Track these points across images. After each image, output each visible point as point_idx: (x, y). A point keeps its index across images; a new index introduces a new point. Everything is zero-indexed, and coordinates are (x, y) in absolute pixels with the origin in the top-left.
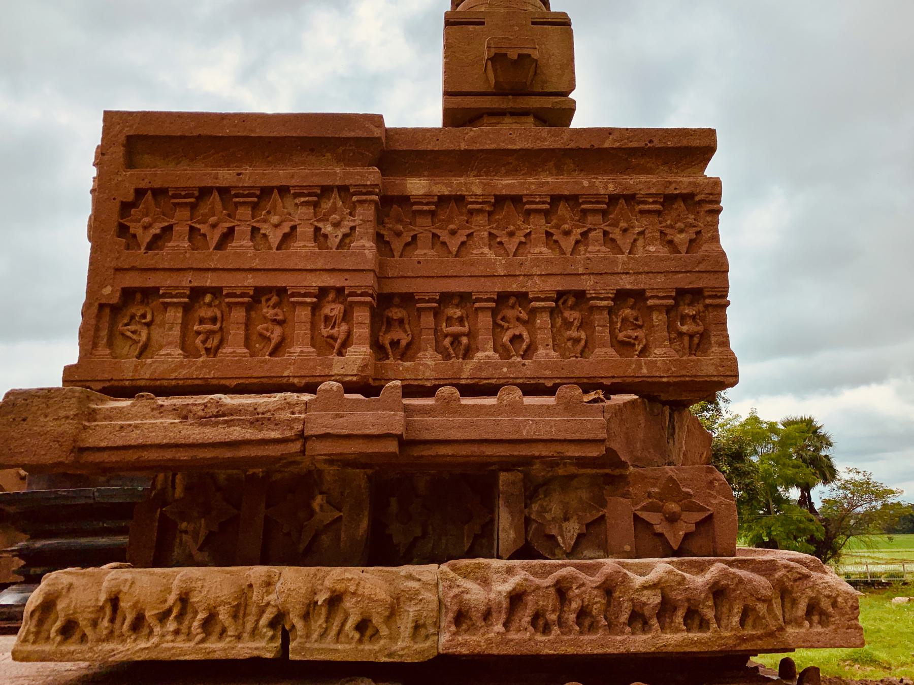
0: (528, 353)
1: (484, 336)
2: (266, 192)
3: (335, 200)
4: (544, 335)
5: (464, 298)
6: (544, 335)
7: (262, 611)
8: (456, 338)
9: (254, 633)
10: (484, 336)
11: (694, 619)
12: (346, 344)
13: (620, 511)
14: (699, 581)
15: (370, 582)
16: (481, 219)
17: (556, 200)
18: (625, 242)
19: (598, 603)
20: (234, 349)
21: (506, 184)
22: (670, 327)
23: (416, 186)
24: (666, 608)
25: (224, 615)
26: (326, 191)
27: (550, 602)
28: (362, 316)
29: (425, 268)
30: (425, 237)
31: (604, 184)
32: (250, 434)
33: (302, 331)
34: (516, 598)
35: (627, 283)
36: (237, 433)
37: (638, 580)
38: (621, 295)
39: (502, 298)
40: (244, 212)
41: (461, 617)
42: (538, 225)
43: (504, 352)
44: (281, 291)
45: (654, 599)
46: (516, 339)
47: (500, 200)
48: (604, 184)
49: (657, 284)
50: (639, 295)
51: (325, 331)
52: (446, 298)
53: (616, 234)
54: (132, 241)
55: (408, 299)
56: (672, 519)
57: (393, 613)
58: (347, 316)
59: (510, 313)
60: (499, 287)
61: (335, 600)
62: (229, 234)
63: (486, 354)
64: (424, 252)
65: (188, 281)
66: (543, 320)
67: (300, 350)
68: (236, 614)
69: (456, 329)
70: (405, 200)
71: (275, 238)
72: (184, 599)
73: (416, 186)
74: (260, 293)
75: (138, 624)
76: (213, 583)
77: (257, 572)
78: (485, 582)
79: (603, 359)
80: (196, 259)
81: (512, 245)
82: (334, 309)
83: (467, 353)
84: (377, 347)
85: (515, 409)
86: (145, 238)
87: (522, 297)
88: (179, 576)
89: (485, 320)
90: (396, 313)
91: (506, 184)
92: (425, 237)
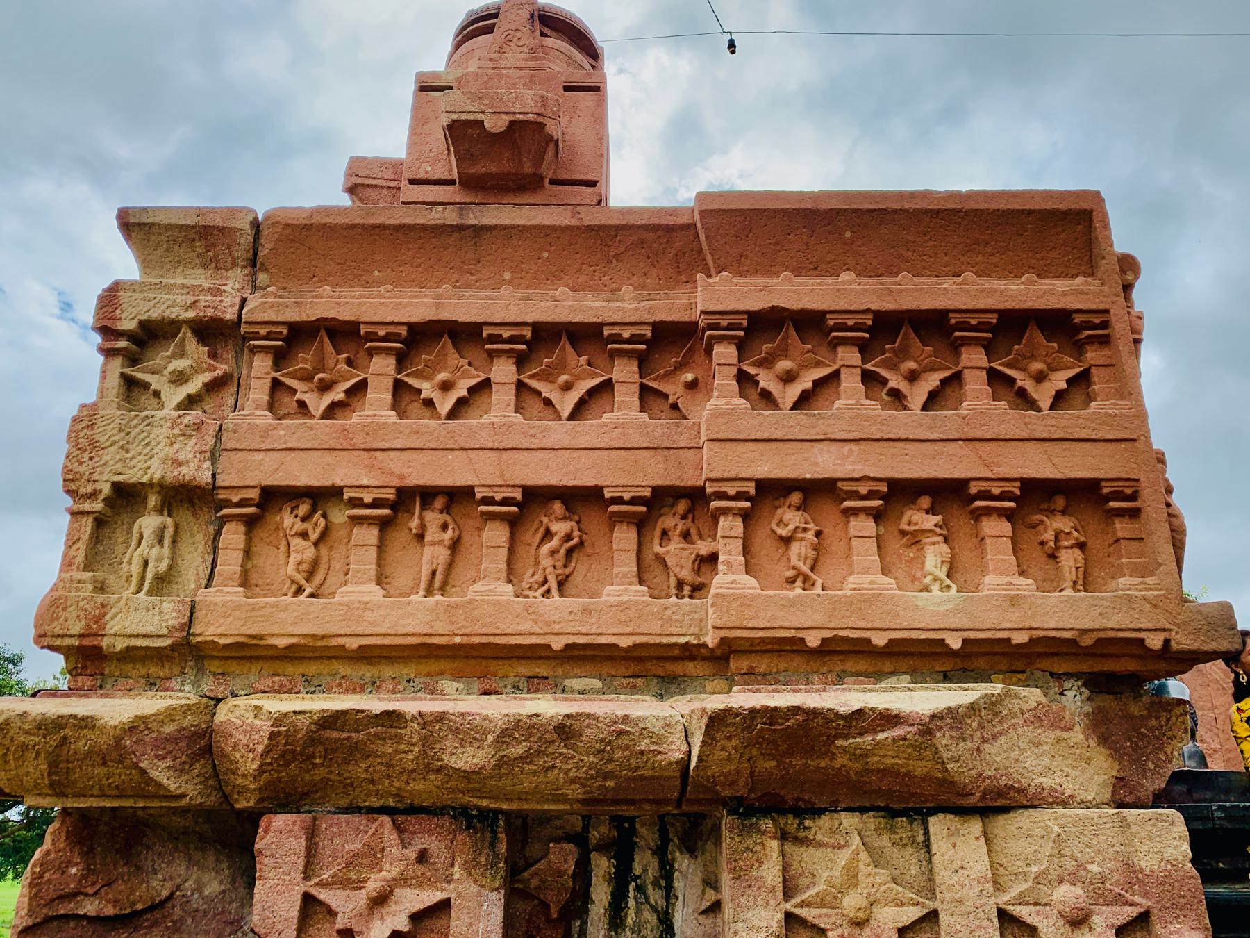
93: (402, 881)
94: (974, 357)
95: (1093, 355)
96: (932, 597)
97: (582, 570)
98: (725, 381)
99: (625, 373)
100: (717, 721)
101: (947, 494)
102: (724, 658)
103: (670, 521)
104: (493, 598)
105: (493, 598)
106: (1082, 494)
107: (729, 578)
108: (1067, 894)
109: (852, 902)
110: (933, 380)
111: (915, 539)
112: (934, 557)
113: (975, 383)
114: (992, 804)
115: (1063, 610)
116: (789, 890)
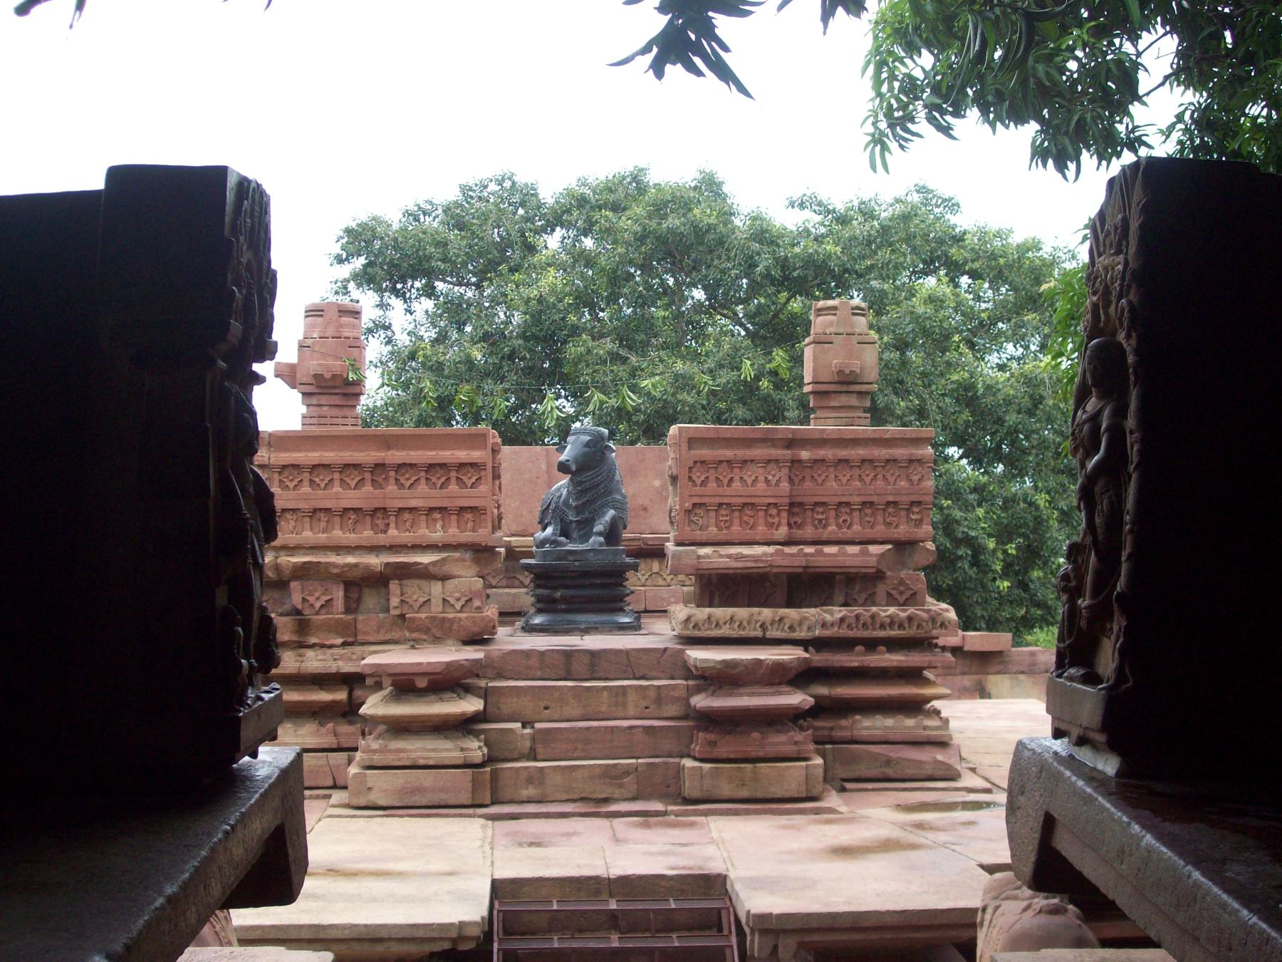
0: (849, 527)
1: (832, 520)
2: (745, 462)
3: (772, 465)
4: (856, 520)
5: (823, 504)
6: (856, 520)
7: (757, 622)
8: (820, 521)
9: (755, 629)
10: (832, 520)
11: (901, 626)
12: (779, 525)
13: (881, 589)
14: (903, 615)
15: (792, 614)
16: (832, 469)
17: (863, 461)
18: (892, 480)
19: (869, 621)
20: (736, 528)
21: (843, 453)
22: (908, 516)
23: (805, 454)
24: (891, 624)
25: (745, 623)
26: (769, 461)
27: (853, 621)
28: (784, 514)
29: (809, 490)
30: (808, 478)
31: (883, 453)
32: (753, 565)
33: (761, 521)
34: (842, 620)
35: (891, 499)
36: (749, 564)
37: (883, 614)
38: (888, 503)
39: (840, 504)
40: (737, 471)
41: (824, 625)
42: (856, 471)
43: (838, 525)
44: (752, 504)
45: (888, 620)
46: (845, 521)
47: (840, 461)
48: (883, 453)
49: (905, 499)
50: (895, 503)
51: (771, 520)
52: (816, 504)
53: (888, 476)
54: (694, 484)
55: (801, 504)
56: (901, 593)
57: (800, 624)
58: (778, 515)
59: (843, 510)
60: (838, 500)
61: (781, 619)
62: (731, 480)
63: (832, 528)
64: (808, 484)
65: (717, 500)
66: (856, 514)
67: (761, 528)
68: (749, 623)
69: (820, 517)
70: (800, 461)
71: (749, 481)
72: (732, 618)
73: (805, 454)
74: (745, 504)
75: (717, 625)
76: (742, 613)
77: (756, 610)
78: (832, 614)
79: (880, 530)
80: (721, 491)
81: (844, 481)
82: (774, 512)
83: (825, 527)
84: (789, 525)
85: (845, 554)
86: (699, 482)
87: (848, 504)
88: (730, 611)
89: (832, 513)
90: (796, 510)
91: (843, 453)
92: (808, 478)
93: (323, 594)
94: (453, 474)
95: (483, 473)
96: (437, 534)
97: (359, 526)
98: (392, 481)
99: (368, 476)
100: (387, 564)
101: (442, 510)
102: (393, 548)
103: (379, 515)
104: (339, 535)
105: (339, 535)
106: (473, 509)
107: (393, 532)
108: (457, 595)
109: (415, 597)
110: (443, 480)
111: (435, 520)
112: (438, 526)
113: (453, 480)
114: (444, 578)
115: (467, 536)
116: (402, 595)
